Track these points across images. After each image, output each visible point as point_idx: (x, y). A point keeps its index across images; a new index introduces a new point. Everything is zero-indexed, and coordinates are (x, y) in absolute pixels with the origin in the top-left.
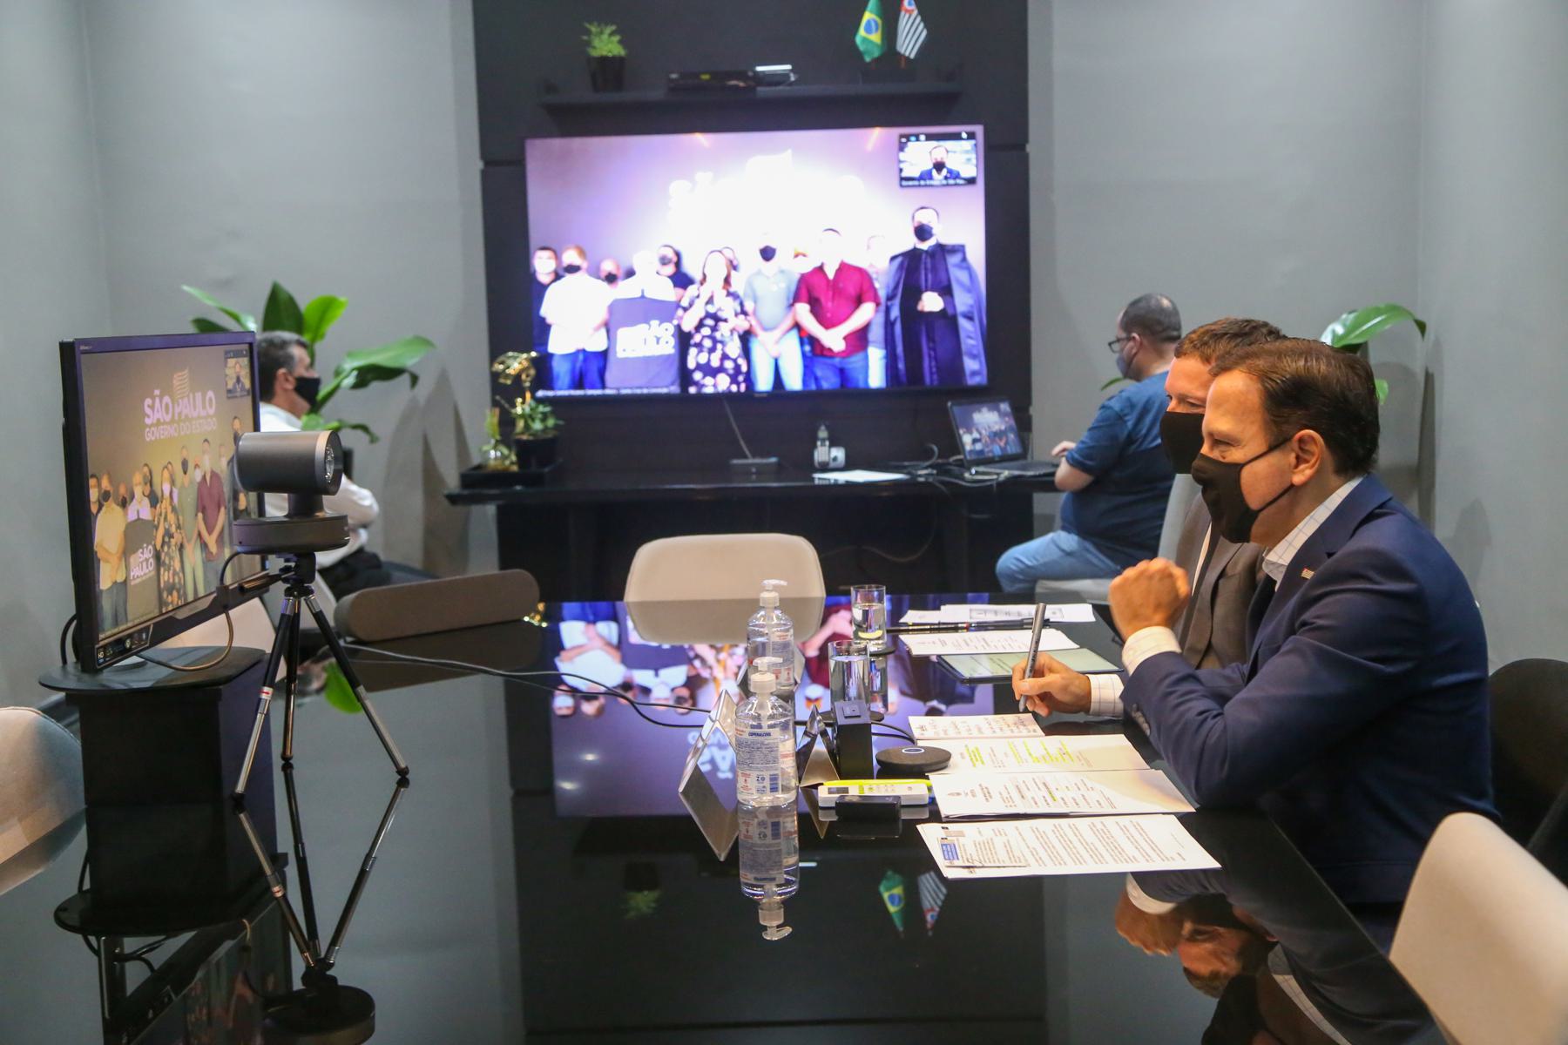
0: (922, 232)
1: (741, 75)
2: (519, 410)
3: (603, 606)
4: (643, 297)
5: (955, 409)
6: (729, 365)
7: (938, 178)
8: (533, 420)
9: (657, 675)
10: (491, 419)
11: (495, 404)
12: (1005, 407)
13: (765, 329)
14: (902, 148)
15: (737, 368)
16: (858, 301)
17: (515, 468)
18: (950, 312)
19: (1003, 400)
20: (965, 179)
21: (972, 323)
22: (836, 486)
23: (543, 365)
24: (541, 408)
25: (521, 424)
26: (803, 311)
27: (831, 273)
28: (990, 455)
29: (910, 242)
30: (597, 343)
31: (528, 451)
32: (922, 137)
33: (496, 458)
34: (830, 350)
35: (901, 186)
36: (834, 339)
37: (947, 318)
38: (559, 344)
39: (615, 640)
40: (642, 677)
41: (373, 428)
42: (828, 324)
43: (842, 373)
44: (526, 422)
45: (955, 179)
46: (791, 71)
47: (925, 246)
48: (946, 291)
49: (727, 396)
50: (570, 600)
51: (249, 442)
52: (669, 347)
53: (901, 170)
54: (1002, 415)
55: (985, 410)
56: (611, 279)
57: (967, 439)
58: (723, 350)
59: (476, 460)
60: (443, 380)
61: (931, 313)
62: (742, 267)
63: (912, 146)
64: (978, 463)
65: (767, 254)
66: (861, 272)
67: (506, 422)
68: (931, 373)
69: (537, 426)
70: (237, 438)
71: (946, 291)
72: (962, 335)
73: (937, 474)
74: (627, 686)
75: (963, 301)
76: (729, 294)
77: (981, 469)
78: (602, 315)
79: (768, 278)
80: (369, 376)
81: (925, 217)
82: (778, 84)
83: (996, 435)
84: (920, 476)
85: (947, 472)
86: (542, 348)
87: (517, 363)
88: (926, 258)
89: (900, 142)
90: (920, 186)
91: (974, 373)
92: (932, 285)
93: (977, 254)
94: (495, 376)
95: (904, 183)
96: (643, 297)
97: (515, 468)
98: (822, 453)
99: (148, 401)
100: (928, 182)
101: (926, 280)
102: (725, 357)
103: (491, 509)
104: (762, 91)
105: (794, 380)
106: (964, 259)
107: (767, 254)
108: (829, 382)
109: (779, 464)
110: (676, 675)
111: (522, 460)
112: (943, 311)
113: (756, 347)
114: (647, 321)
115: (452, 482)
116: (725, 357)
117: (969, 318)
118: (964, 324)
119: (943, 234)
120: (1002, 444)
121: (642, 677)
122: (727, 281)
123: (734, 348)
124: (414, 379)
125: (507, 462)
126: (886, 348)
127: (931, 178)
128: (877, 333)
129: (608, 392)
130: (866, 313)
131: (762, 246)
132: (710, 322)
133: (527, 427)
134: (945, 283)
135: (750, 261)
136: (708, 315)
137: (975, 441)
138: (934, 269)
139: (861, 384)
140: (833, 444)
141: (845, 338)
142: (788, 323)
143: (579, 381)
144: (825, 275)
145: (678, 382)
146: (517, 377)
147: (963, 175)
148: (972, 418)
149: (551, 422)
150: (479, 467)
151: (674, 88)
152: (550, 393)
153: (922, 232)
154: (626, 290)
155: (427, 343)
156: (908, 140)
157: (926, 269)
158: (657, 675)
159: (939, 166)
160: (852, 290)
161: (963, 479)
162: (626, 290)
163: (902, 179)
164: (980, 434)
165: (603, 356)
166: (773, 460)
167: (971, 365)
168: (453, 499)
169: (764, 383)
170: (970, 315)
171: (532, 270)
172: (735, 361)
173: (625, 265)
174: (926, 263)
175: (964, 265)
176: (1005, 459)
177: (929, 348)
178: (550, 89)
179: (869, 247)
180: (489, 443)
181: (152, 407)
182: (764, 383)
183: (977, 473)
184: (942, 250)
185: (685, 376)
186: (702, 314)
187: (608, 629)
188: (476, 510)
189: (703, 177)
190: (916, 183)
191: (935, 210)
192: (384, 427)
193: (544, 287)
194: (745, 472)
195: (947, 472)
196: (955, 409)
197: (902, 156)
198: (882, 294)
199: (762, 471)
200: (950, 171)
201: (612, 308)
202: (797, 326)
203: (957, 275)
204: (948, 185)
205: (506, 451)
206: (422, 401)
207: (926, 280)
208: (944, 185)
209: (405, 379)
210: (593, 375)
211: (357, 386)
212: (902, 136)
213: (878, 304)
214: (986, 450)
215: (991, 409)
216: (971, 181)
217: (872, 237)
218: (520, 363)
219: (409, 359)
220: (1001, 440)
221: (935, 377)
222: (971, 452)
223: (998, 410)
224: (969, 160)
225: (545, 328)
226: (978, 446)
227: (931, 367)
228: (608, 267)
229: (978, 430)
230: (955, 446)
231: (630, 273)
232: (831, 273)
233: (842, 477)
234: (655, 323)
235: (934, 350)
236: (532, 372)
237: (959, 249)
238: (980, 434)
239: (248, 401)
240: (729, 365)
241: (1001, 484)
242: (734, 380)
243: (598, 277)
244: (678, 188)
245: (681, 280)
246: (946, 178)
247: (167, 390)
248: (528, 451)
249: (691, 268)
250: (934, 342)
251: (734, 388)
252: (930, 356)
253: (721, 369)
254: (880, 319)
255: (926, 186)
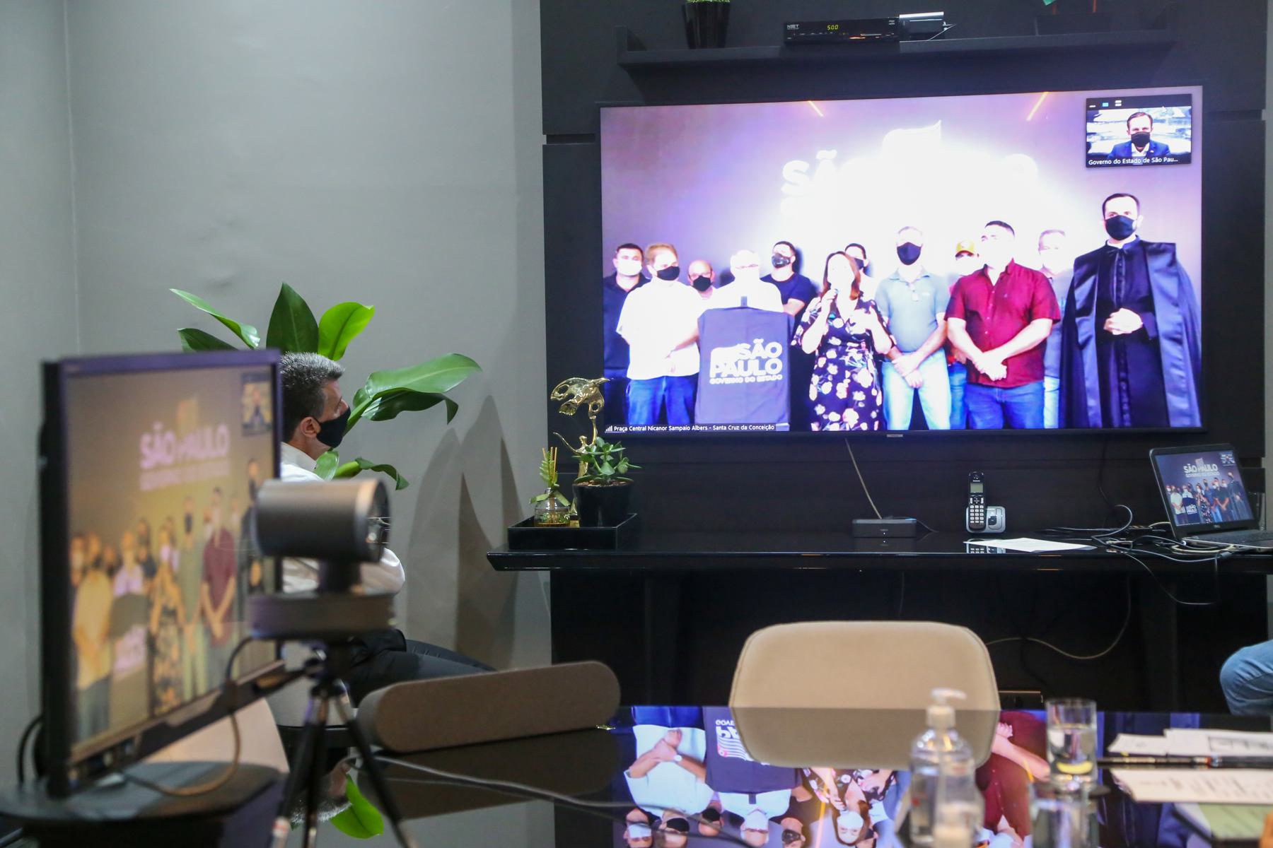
0: (1117, 226)
1: (880, 24)
2: (583, 450)
3: (684, 710)
4: (744, 307)
5: (1160, 461)
6: (859, 396)
7: (1138, 154)
8: (601, 464)
9: (753, 801)
10: (547, 462)
11: (553, 441)
12: (1227, 457)
13: (902, 351)
14: (1090, 118)
15: (870, 400)
16: (1028, 317)
17: (576, 524)
18: (1151, 333)
19: (1225, 450)
20: (1174, 156)
21: (1179, 347)
22: (994, 556)
23: (616, 393)
24: (611, 448)
25: (584, 468)
26: (957, 326)
27: (994, 277)
28: (1209, 521)
29: (1097, 238)
30: (686, 364)
31: (590, 501)
32: (1118, 103)
33: (552, 511)
34: (985, 376)
35: (1088, 166)
36: (992, 364)
37: (1146, 340)
38: (641, 368)
39: (701, 752)
40: (733, 802)
41: (400, 471)
42: (985, 344)
43: (1007, 411)
44: (591, 465)
45: (1162, 156)
46: (944, 18)
47: (1119, 245)
48: (1145, 306)
49: (854, 436)
50: (641, 702)
51: (270, 493)
52: (775, 371)
53: (1088, 146)
54: (1223, 468)
55: (1199, 461)
56: (702, 284)
57: (1176, 499)
58: (851, 378)
59: (527, 513)
60: (489, 409)
61: (1124, 336)
62: (875, 270)
63: (1105, 115)
64: (1191, 532)
65: (908, 254)
66: (1036, 280)
67: (567, 465)
68: (1122, 412)
69: (607, 470)
70: (253, 490)
71: (1145, 306)
72: (1166, 361)
73: (1135, 545)
74: (712, 813)
75: (1167, 319)
76: (861, 305)
77: (1196, 540)
78: (692, 329)
79: (908, 284)
80: (398, 404)
81: (1119, 207)
82: (928, 35)
83: (1217, 495)
84: (1109, 547)
85: (1148, 544)
86: (619, 372)
87: (581, 390)
88: (1120, 260)
89: (1088, 109)
90: (1113, 165)
91: (1182, 413)
92: (1127, 296)
93: (1190, 257)
94: (553, 406)
95: (1092, 162)
96: (744, 307)
97: (576, 524)
98: (974, 514)
99: (146, 439)
100: (1128, 161)
101: (1119, 289)
102: (854, 386)
103: (544, 576)
104: (906, 45)
105: (940, 418)
106: (1173, 262)
107: (908, 254)
108: (986, 420)
109: (918, 526)
110: (776, 801)
111: (586, 513)
112: (1141, 333)
113: (890, 374)
114: (748, 340)
115: (496, 540)
116: (854, 386)
117: (1178, 342)
118: (1166, 345)
119: (1146, 229)
120: (1223, 507)
121: (733, 802)
122: (855, 285)
123: (865, 377)
124: (453, 409)
125: (567, 516)
126: (1061, 378)
127: (1129, 156)
128: (1052, 358)
129: (696, 428)
130: (1039, 330)
131: (901, 243)
132: (835, 341)
133: (592, 471)
134: (1144, 293)
135: (884, 261)
136: (833, 332)
137: (1186, 502)
138: (1130, 275)
139: (1029, 424)
140: (988, 503)
141: (1005, 362)
142: (936, 340)
143: (660, 413)
144: (988, 280)
145: (786, 417)
146: (583, 407)
147: (1173, 150)
148: (1183, 473)
149: (623, 466)
150: (530, 522)
151: (793, 43)
152: (623, 430)
153: (1117, 226)
154: (722, 298)
155: (470, 362)
156: (1100, 107)
157: (1119, 274)
158: (753, 801)
159: (1140, 139)
160: (1020, 300)
161: (1170, 552)
162: (722, 298)
163: (1090, 157)
164: (1194, 493)
165: (692, 382)
166: (910, 520)
167: (1178, 403)
168: (498, 562)
169: (900, 420)
170: (1178, 336)
171: (607, 273)
172: (867, 391)
173: (720, 268)
174: (1119, 267)
175: (1172, 270)
176: (1229, 527)
177: (1120, 380)
178: (635, 44)
179: (1041, 247)
180: (546, 492)
181: (151, 445)
182: (900, 420)
183: (1189, 544)
184: (1145, 250)
185: (800, 408)
186: (825, 331)
187: (694, 739)
188: (524, 576)
189: (825, 156)
190: (1109, 162)
191: (1132, 197)
192: (413, 468)
193: (622, 294)
194: (874, 535)
195: (1148, 544)
196: (1160, 461)
197: (1091, 127)
198: (1061, 304)
199: (895, 535)
200: (1155, 147)
201: (704, 321)
202: (947, 346)
203: (1163, 283)
204: (1151, 164)
205: (565, 503)
206: (461, 435)
207: (1119, 289)
208: (1145, 165)
209: (442, 407)
210: (678, 407)
211: (379, 417)
212: (1089, 101)
213: (1055, 322)
214: (1202, 514)
215: (1207, 461)
216: (1184, 159)
217: (1047, 232)
218: (586, 390)
219: (447, 385)
220: (1222, 502)
221: (1127, 416)
222: (1180, 516)
223: (1218, 462)
224: (1181, 131)
225: (622, 348)
226: (1191, 510)
227: (1121, 405)
228: (698, 269)
229: (1190, 487)
230: (1160, 508)
231: (727, 278)
232: (994, 277)
233: (1002, 545)
234: (758, 342)
235: (1126, 380)
236: (601, 402)
237: (1168, 249)
238: (1194, 493)
239: (267, 439)
240: (859, 396)
241: (1223, 561)
242: (864, 415)
243: (688, 284)
244: (793, 169)
245: (798, 288)
246: (1149, 155)
247: (171, 424)
248: (590, 501)
249: (811, 271)
250: (1126, 371)
251: (864, 426)
252: (1120, 389)
253: (848, 403)
254: (1055, 341)
255: (1121, 165)
